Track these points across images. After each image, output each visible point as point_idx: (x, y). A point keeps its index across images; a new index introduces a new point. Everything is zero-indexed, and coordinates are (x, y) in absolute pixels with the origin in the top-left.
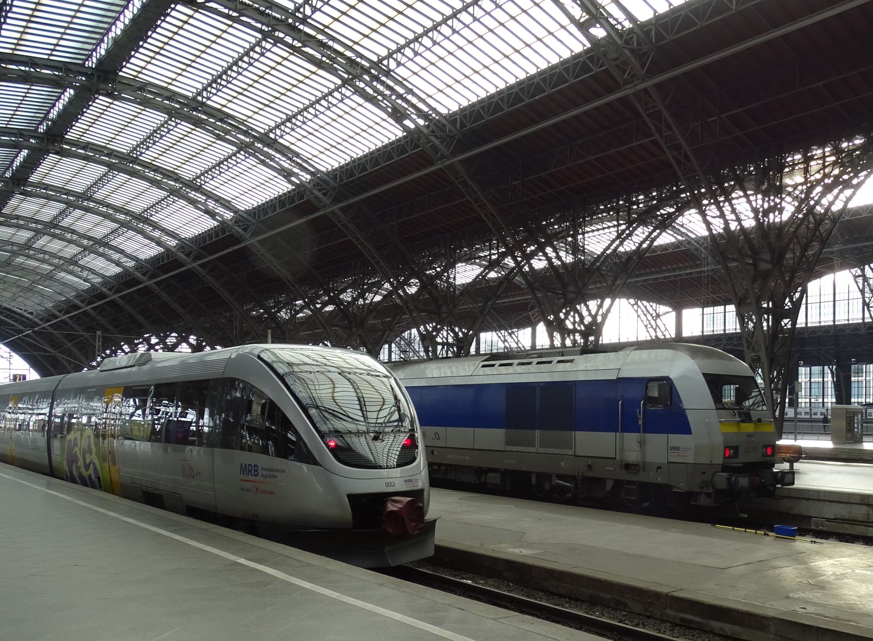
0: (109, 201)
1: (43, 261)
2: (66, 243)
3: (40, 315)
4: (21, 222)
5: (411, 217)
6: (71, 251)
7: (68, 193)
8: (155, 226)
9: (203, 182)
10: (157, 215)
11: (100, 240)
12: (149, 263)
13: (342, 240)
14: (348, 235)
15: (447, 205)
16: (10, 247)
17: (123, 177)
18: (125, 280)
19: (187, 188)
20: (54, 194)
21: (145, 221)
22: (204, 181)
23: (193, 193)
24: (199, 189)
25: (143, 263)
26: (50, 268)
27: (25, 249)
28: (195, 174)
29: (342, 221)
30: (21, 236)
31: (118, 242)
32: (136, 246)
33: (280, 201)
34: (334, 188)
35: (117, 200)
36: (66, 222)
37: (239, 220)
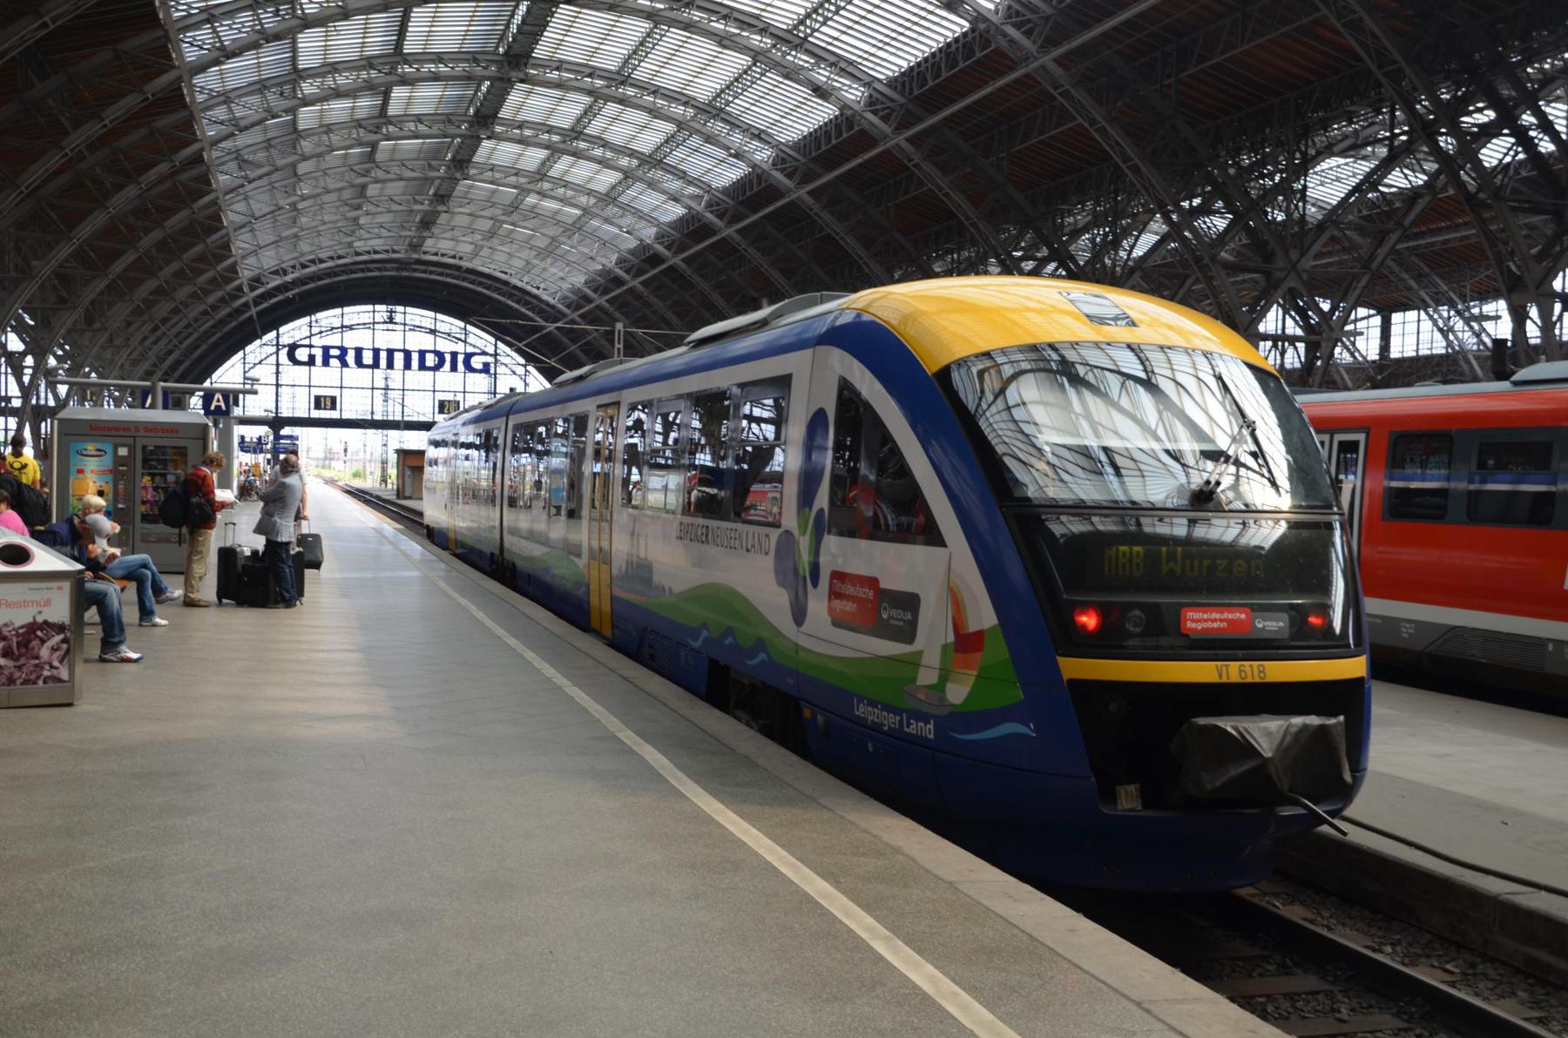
0: (659, 82)
1: (563, 201)
2: (596, 166)
3: (566, 298)
4: (528, 132)
5: (1209, 64)
6: (608, 178)
7: (593, 72)
8: (734, 123)
9: (808, 31)
10: (736, 101)
11: (650, 156)
12: (728, 195)
13: (1070, 125)
14: (1078, 117)
15: (1283, 30)
16: (513, 179)
17: (676, 34)
18: (690, 230)
19: (782, 45)
20: (573, 76)
21: (718, 115)
22: (810, 27)
23: (793, 53)
24: (801, 45)
25: (719, 195)
26: (577, 212)
27: (538, 181)
28: (796, 17)
29: (1063, 86)
30: (532, 157)
31: (676, 157)
32: (707, 164)
33: (948, 55)
34: (1047, 18)
35: (671, 79)
36: (595, 127)
37: (877, 99)
